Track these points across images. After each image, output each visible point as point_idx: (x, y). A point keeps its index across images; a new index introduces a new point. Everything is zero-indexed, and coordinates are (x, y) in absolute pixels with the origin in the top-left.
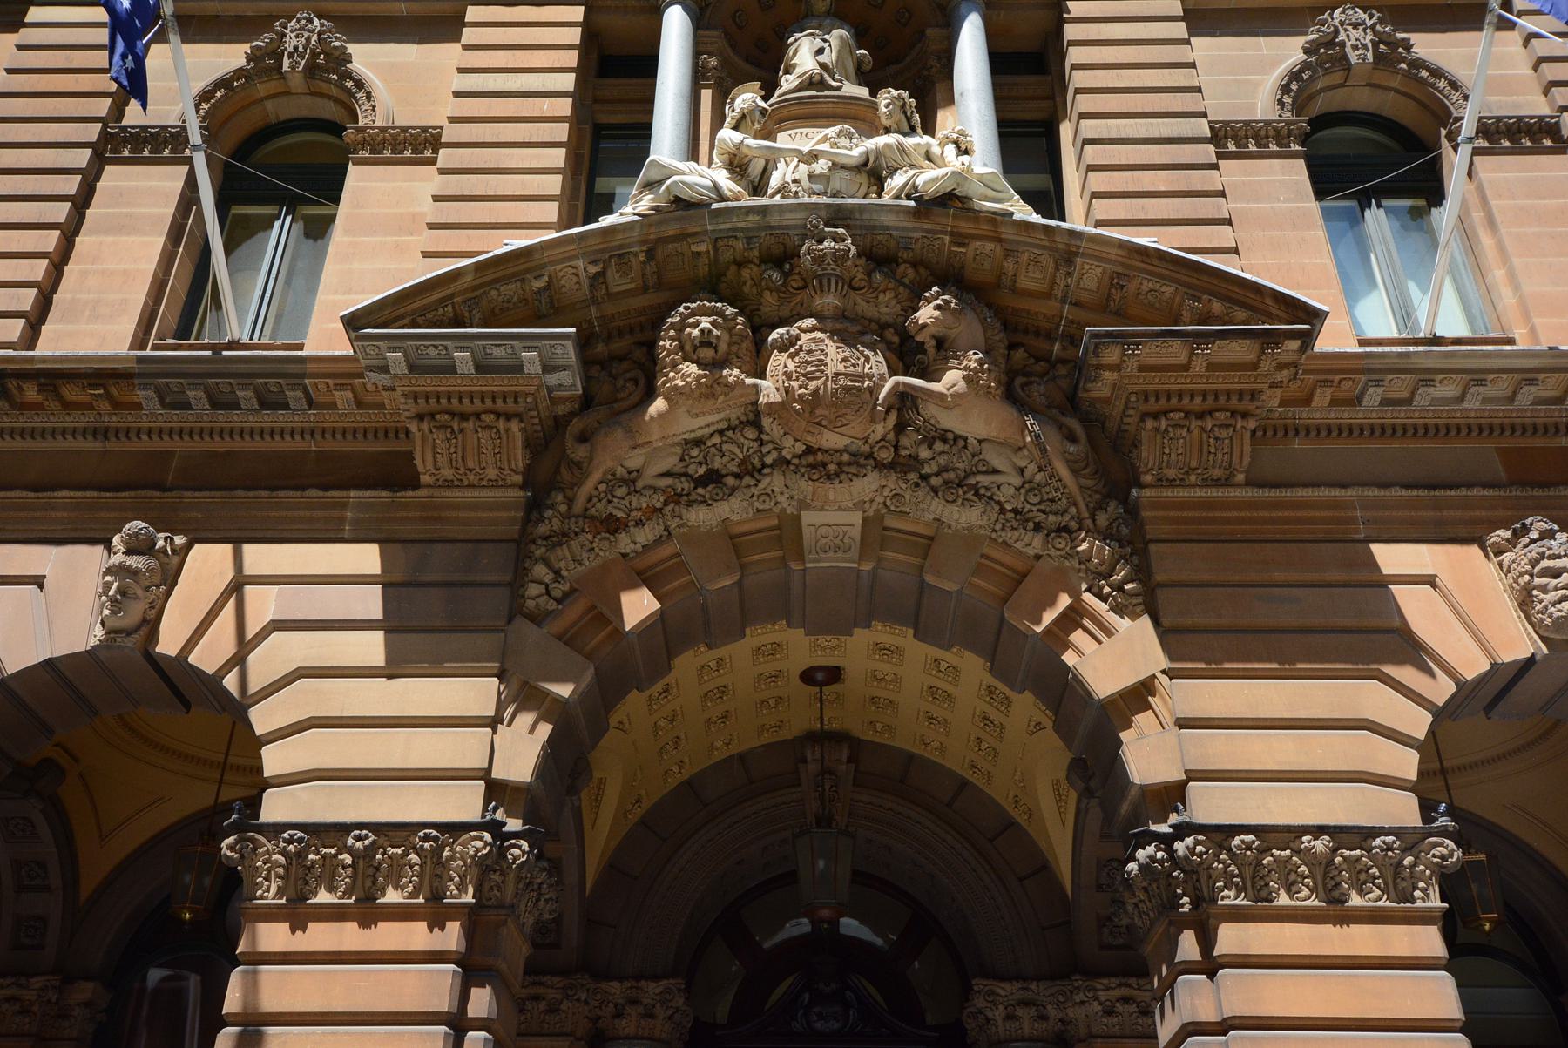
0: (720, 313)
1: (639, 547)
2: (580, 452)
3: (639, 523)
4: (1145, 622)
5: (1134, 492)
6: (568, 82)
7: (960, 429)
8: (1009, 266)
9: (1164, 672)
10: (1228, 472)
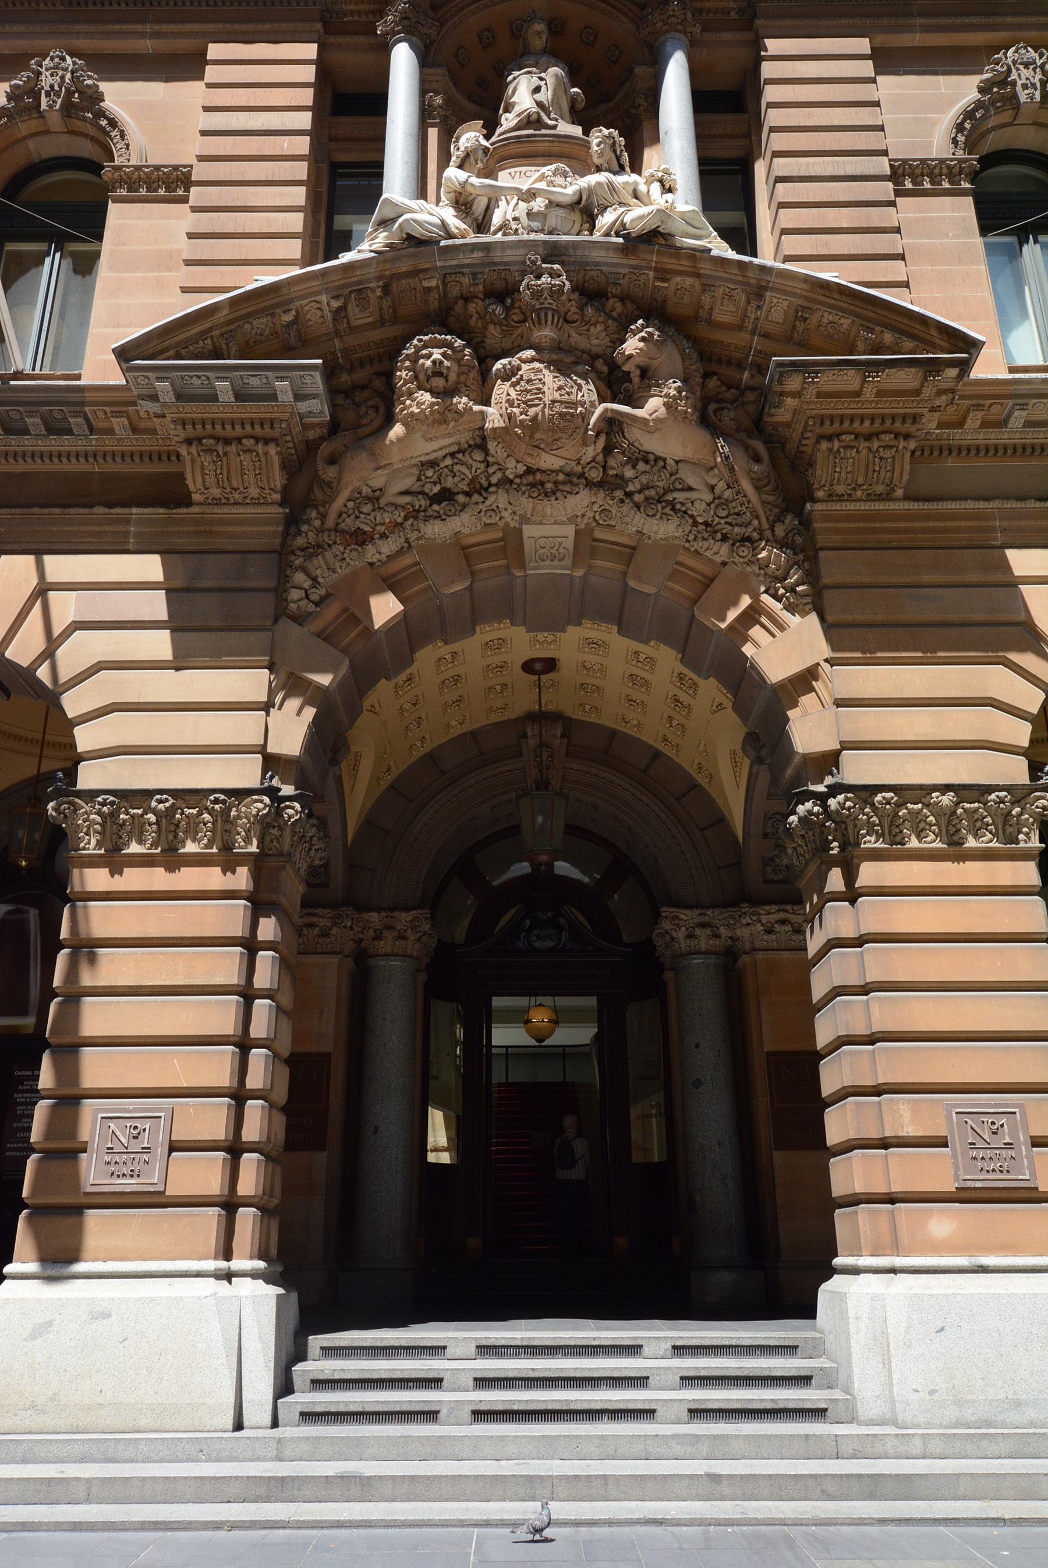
0: (449, 345)
1: (383, 557)
2: (330, 473)
3: (383, 536)
4: (813, 618)
5: (808, 506)
6: (304, 121)
7: (660, 451)
8: (706, 299)
9: (826, 660)
10: (889, 488)
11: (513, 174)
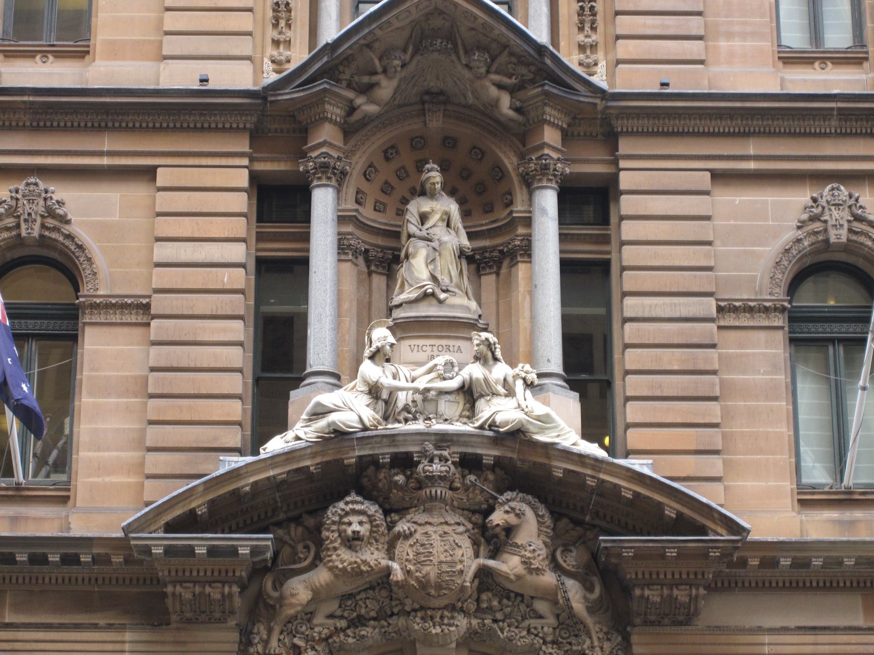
11: (412, 347)
